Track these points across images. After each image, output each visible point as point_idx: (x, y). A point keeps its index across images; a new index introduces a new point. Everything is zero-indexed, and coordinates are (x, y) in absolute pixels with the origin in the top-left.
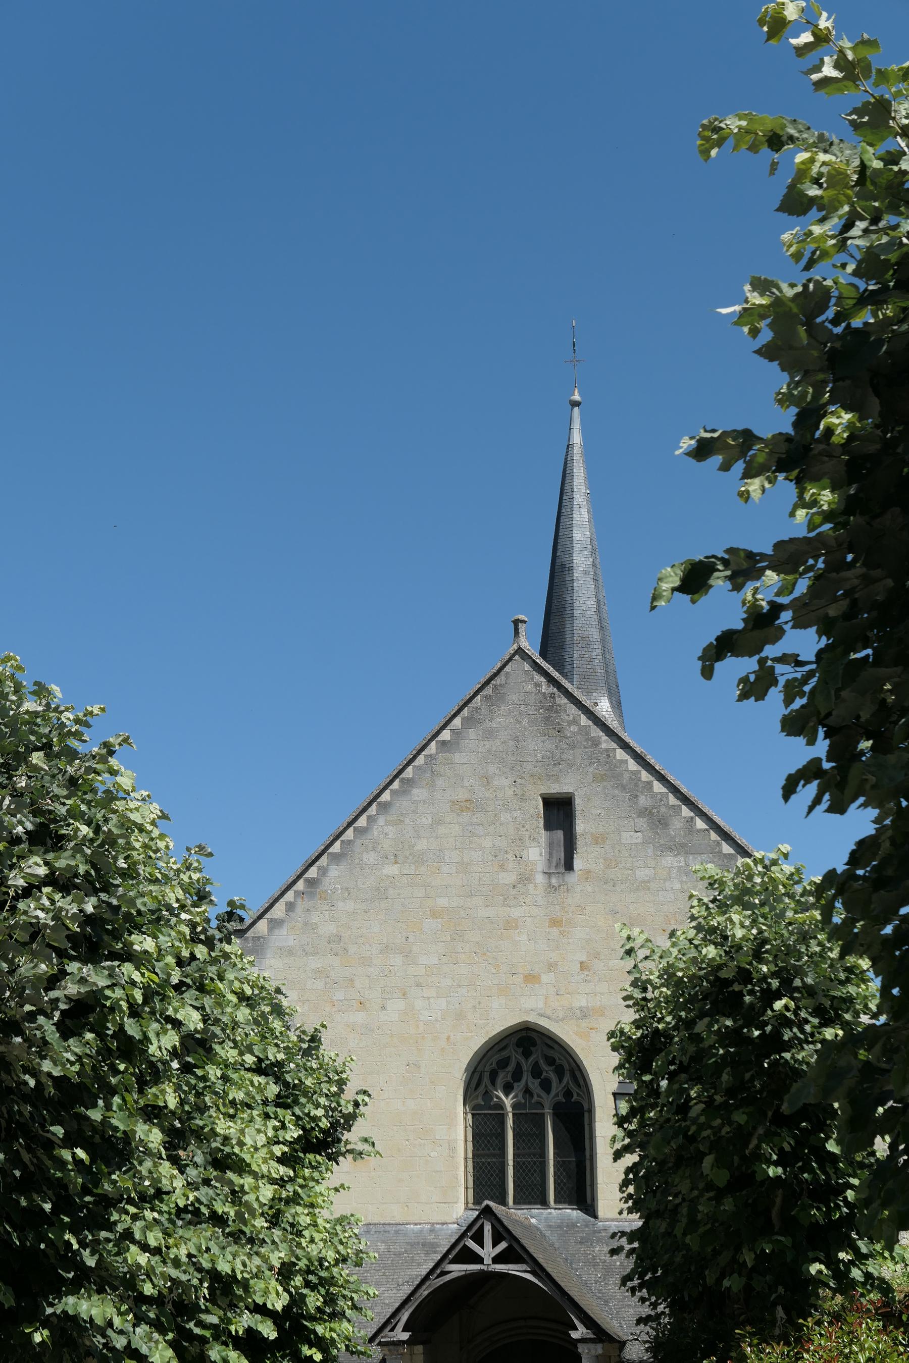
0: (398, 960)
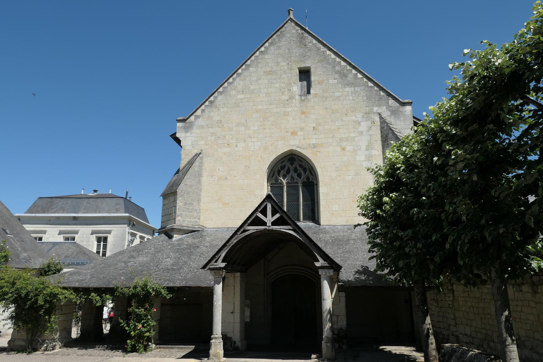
0: (243, 128)
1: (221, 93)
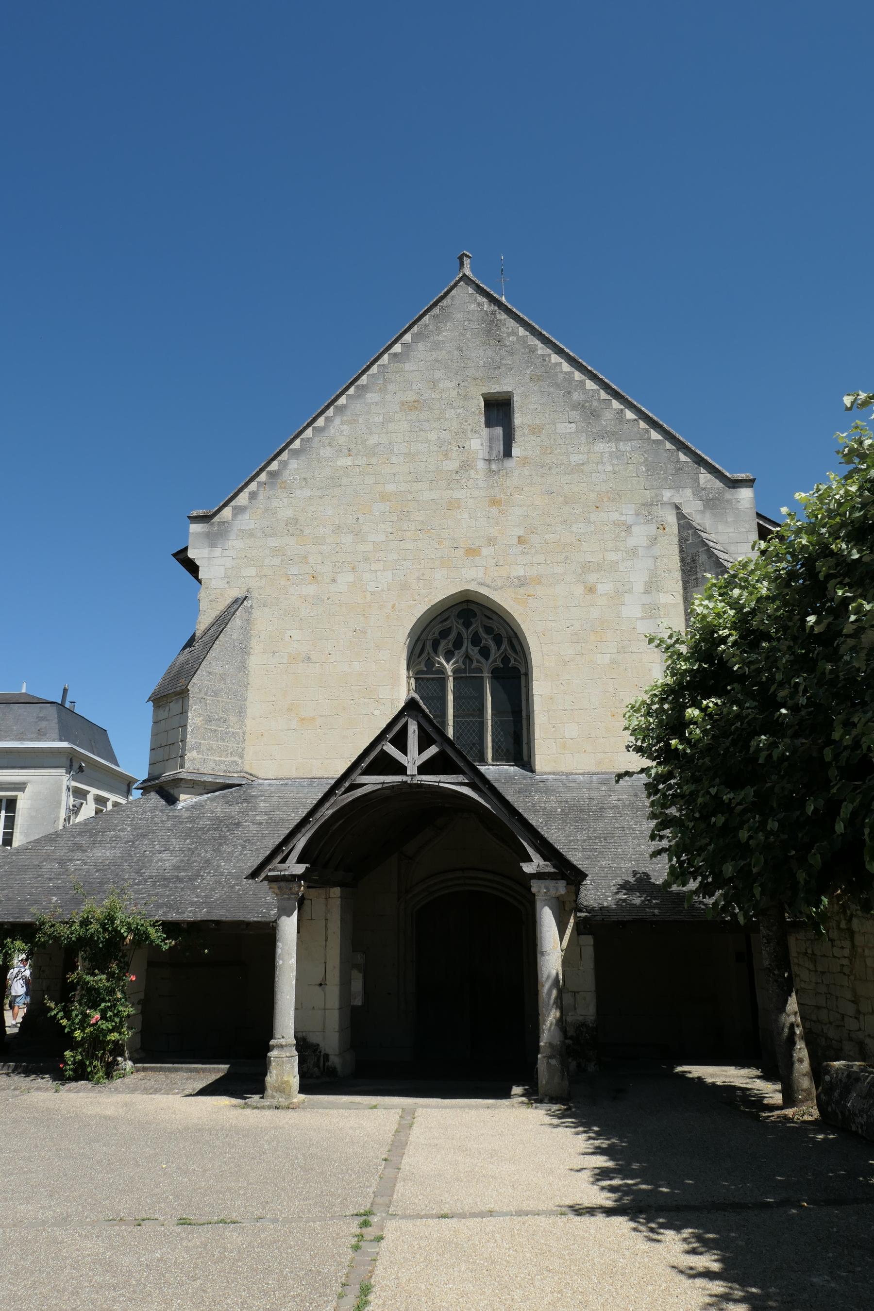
0: (349, 539)
1: (296, 453)
